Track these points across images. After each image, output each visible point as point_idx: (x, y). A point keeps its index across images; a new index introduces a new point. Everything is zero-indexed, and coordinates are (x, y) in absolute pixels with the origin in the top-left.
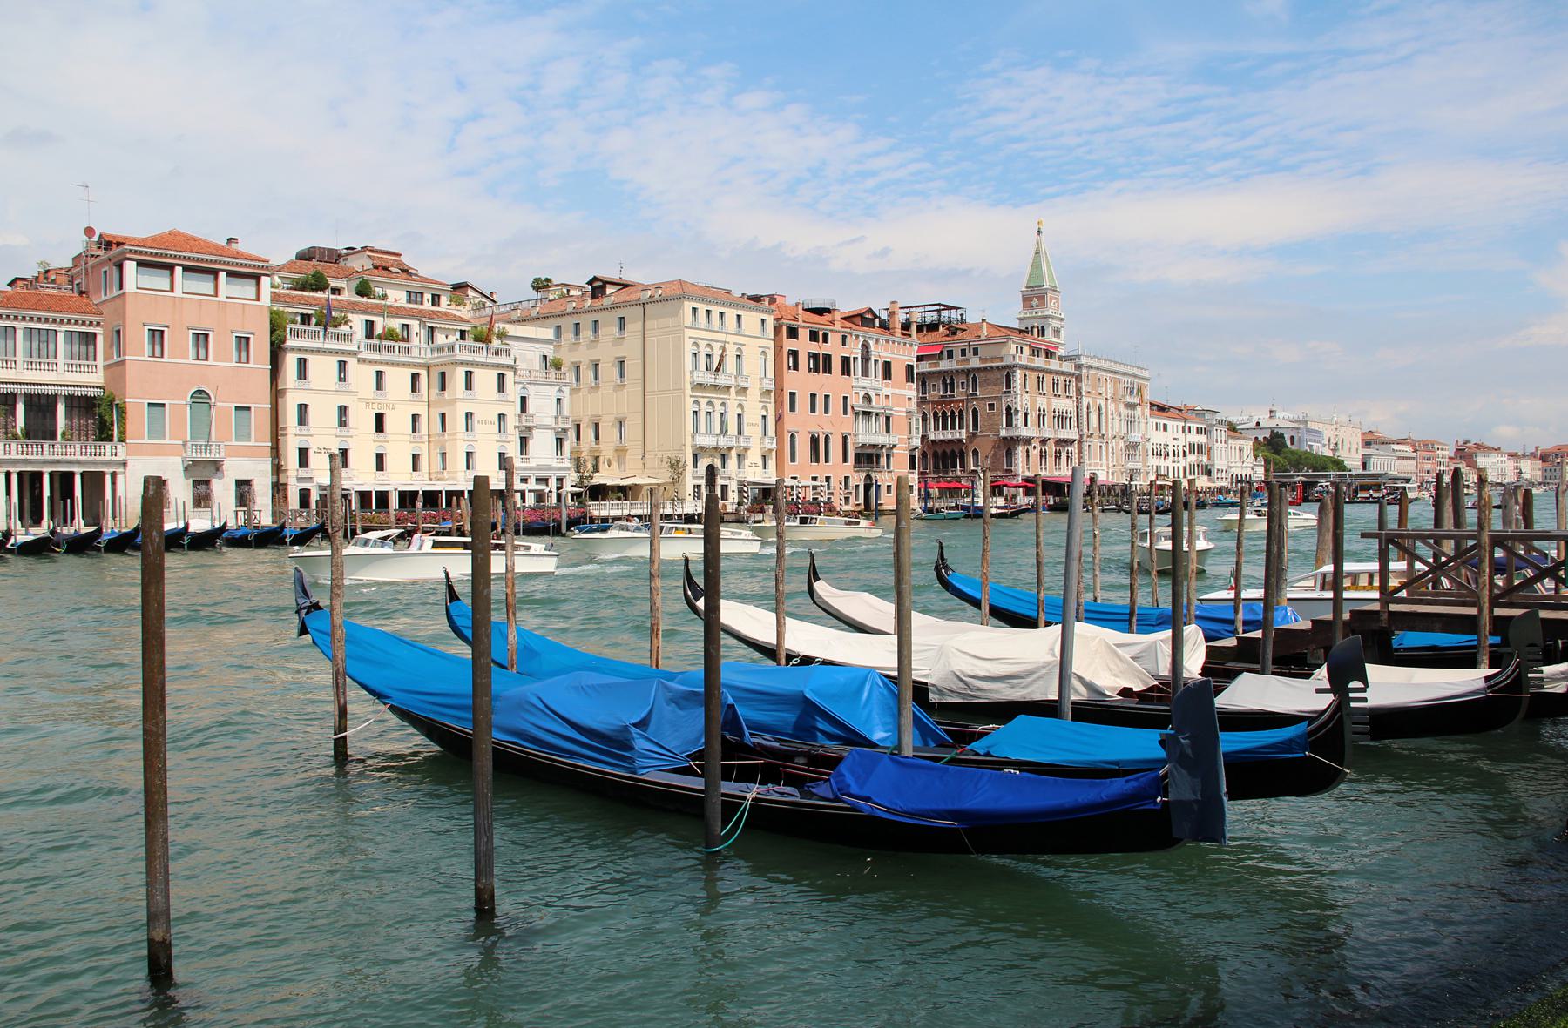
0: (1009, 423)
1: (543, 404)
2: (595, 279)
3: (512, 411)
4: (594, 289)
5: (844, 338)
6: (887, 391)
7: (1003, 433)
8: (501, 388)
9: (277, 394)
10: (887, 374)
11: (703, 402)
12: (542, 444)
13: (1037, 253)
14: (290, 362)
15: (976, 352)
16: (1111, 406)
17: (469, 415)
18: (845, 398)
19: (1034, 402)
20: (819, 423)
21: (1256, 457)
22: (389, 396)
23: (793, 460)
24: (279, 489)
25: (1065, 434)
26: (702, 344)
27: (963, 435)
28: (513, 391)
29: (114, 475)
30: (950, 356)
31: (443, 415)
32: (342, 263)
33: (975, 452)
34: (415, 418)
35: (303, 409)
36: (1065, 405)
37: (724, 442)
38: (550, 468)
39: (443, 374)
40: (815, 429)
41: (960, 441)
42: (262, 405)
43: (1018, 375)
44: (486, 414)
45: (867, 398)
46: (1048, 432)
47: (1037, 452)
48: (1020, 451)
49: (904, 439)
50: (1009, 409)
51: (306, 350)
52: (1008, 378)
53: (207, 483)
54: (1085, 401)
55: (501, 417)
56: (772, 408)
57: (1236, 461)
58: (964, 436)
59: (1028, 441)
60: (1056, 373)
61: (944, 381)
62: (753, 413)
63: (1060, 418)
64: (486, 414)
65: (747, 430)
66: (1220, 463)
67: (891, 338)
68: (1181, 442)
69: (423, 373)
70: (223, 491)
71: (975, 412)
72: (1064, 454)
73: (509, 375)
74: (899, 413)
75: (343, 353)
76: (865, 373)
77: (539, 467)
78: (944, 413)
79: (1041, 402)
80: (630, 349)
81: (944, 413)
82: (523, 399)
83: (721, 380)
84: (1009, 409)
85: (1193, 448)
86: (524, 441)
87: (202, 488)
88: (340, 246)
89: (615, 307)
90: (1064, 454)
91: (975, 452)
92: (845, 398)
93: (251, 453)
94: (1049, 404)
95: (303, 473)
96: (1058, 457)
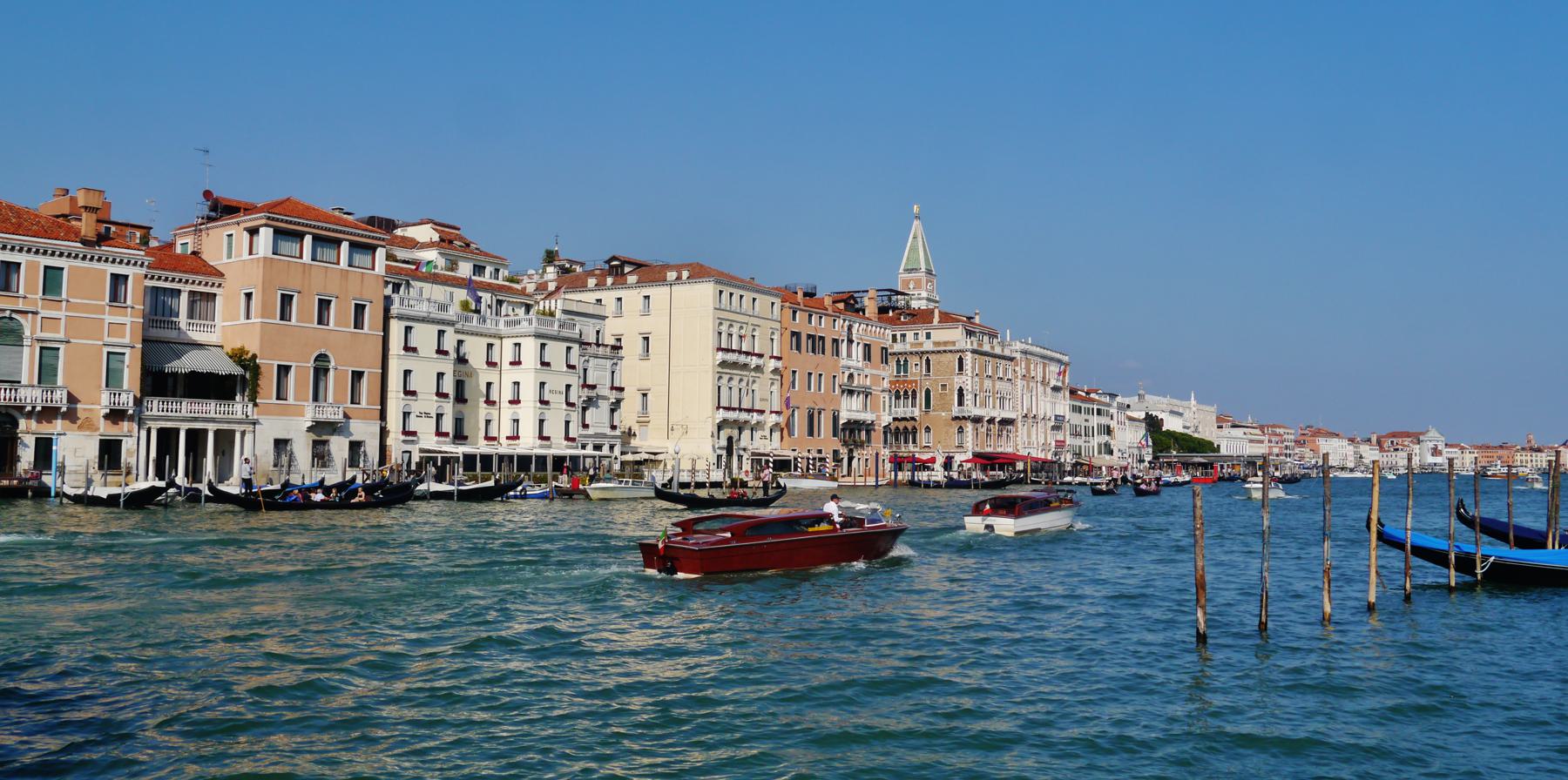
0: (961, 403)
2: (614, 258)
6: (867, 371)
10: (867, 356)
14: (396, 328)
15: (928, 336)
16: (1040, 388)
19: (982, 384)
27: (916, 413)
29: (243, 433)
31: (517, 384)
32: (399, 232)
33: (928, 429)
39: (518, 345)
41: (913, 419)
42: (371, 372)
43: (968, 358)
45: (851, 376)
47: (984, 430)
50: (961, 391)
52: (961, 360)
53: (325, 442)
59: (977, 420)
70: (338, 447)
71: (928, 392)
76: (849, 355)
77: (597, 435)
79: (988, 383)
80: (655, 324)
84: (961, 391)
87: (320, 448)
91: (928, 429)
93: (364, 416)
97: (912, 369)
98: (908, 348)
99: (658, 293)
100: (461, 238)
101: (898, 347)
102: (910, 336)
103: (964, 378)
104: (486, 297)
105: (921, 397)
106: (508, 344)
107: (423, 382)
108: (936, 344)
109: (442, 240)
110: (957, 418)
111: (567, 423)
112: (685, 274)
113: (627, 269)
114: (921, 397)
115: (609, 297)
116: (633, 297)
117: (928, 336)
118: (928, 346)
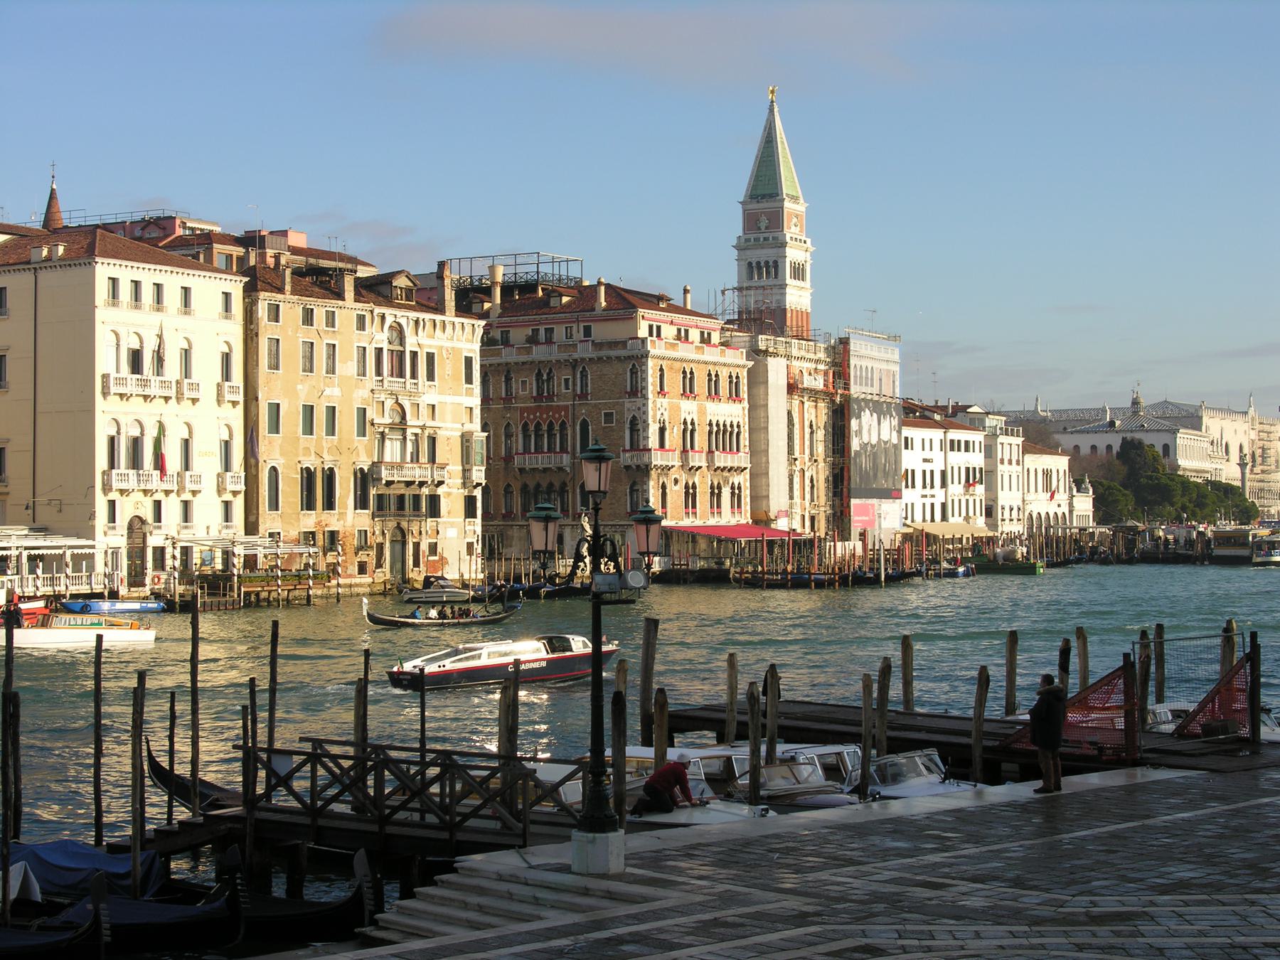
5: (361, 319)
15: (587, 331)
18: (362, 412)
20: (317, 452)
21: (1079, 484)
23: (274, 505)
36: (732, 412)
40: (310, 462)
41: (560, 469)
47: (680, 488)
52: (634, 372)
58: (566, 459)
60: (715, 364)
61: (539, 375)
63: (723, 436)
67: (438, 318)
68: (938, 467)
71: (584, 425)
72: (726, 492)
78: (538, 426)
79: (689, 409)
81: (538, 426)
84: (634, 422)
90: (726, 492)
92: (362, 412)
94: (702, 412)
96: (715, 493)
97: (558, 386)
98: (554, 354)
101: (539, 353)
102: (559, 333)
103: (639, 401)
108: (598, 346)
110: (627, 468)
117: (587, 331)
118: (585, 351)
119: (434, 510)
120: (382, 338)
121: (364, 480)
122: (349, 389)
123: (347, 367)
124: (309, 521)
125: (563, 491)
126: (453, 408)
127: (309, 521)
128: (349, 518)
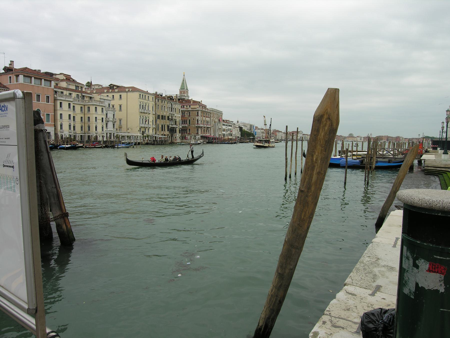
1: (110, 116)
2: (111, 85)
3: (104, 117)
4: (110, 87)
6: (175, 115)
7: (196, 125)
8: (102, 111)
9: (55, 110)
11: (142, 116)
12: (110, 125)
13: (183, 80)
15: (190, 106)
17: (96, 118)
22: (76, 112)
24: (56, 134)
25: (208, 126)
26: (142, 103)
28: (105, 112)
30: (184, 108)
31: (89, 118)
32: (54, 76)
33: (189, 129)
34: (82, 118)
35: (61, 114)
36: (208, 119)
37: (146, 126)
38: (112, 131)
39: (89, 108)
42: (52, 114)
43: (200, 112)
44: (99, 118)
46: (205, 126)
48: (200, 129)
49: (179, 127)
51: (62, 100)
52: (198, 113)
54: (212, 118)
55: (102, 118)
56: (154, 118)
57: (236, 133)
59: (202, 127)
62: (151, 120)
64: (99, 118)
65: (150, 123)
66: (234, 133)
69: (83, 106)
71: (190, 120)
73: (104, 108)
74: (178, 120)
75: (70, 101)
77: (110, 131)
79: (204, 118)
80: (123, 102)
82: (107, 114)
83: (145, 112)
85: (229, 130)
86: (107, 124)
88: (54, 72)
89: (118, 92)
93: (50, 125)
95: (61, 131)
97: (186, 114)
98: (185, 109)
99: (124, 95)
100: (72, 79)
101: (182, 109)
102: (185, 107)
104: (80, 94)
105: (188, 122)
106: (86, 107)
107: (65, 117)
109: (66, 79)
111: (102, 127)
112: (131, 90)
113: (115, 87)
114: (188, 122)
115: (110, 95)
116: (117, 96)
117: (190, 106)
118: (190, 109)
119: (176, 132)
120: (170, 105)
121: (168, 126)
122: (166, 113)
123: (166, 110)
124: (162, 133)
125: (186, 130)
126: (178, 116)
127: (162, 133)
128: (167, 132)
